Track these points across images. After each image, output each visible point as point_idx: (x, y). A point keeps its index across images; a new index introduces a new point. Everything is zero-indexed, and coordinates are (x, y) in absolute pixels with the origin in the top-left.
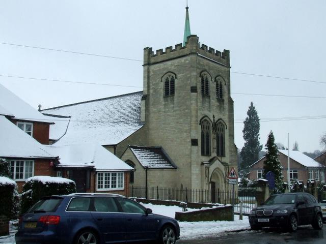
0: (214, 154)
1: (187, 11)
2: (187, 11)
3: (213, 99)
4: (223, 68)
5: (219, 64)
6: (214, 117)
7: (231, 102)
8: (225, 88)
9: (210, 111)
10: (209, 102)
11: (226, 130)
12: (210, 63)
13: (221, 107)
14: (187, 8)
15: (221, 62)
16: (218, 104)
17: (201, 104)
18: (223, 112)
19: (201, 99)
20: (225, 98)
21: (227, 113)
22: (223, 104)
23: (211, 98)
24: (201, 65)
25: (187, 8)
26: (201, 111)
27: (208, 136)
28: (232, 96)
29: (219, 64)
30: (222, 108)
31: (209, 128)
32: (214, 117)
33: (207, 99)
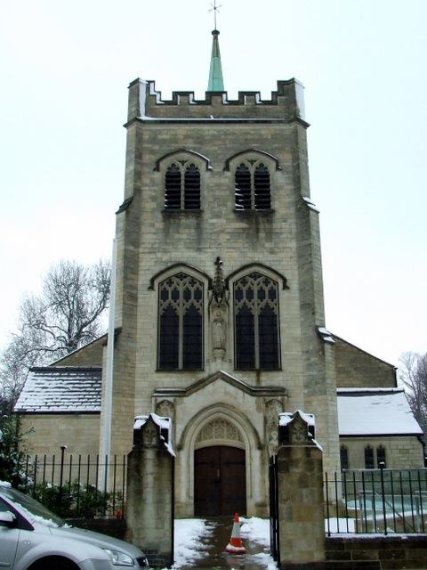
0: (218, 363)
1: (216, 39)
2: (216, 39)
3: (218, 216)
4: (287, 129)
5: (246, 122)
6: (218, 263)
7: (305, 215)
8: (279, 180)
9: (199, 250)
10: (199, 227)
11: (283, 295)
12: (205, 127)
13: (258, 231)
14: (216, 33)
15: (257, 116)
16: (244, 225)
17: (161, 236)
18: (268, 245)
19: (160, 225)
20: (282, 203)
21: (293, 244)
22: (270, 222)
23: (207, 215)
24: (164, 141)
25: (216, 33)
26: (159, 255)
27: (194, 322)
28: (316, 198)
29: (246, 122)
30: (262, 235)
31: (199, 295)
32: (218, 263)
33: (187, 221)
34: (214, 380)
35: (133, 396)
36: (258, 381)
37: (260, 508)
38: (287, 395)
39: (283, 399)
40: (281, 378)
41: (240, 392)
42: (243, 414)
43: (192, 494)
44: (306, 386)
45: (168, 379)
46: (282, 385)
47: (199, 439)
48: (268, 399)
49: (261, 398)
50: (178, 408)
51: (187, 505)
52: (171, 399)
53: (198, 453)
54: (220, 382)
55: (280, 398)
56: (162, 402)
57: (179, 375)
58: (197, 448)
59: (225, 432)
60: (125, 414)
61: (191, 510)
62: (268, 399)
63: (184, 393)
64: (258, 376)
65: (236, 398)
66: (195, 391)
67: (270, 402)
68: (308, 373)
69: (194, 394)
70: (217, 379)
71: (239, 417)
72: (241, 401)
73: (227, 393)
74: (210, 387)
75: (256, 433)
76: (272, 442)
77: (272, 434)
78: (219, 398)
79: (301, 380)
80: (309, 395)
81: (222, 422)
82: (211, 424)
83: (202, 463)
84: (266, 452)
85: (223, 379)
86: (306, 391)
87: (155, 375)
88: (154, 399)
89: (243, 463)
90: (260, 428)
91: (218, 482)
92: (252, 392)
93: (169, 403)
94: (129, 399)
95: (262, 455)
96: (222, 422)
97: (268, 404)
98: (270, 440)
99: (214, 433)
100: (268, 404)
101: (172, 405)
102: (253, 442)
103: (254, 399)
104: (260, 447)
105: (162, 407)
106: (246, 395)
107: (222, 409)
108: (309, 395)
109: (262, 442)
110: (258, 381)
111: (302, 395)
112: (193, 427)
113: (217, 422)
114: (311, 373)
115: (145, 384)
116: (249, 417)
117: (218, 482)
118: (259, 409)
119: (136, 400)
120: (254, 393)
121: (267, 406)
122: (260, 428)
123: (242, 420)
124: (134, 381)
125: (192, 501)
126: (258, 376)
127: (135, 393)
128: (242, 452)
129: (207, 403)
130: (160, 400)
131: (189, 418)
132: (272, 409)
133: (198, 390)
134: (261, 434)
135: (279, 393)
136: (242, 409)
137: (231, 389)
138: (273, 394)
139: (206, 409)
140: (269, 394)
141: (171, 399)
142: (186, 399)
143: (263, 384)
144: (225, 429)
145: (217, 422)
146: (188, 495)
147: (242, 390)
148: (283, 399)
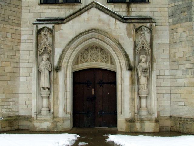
34: (89, 9)
35: (19, 25)
36: (128, 11)
37: (130, 124)
38: (155, 22)
39: (151, 26)
40: (148, 9)
41: (113, 20)
42: (115, 39)
43: (70, 109)
44: (171, 16)
45: (50, 11)
46: (150, 15)
47: (76, 62)
48: (138, 25)
49: (132, 25)
50: (57, 34)
51: (64, 120)
52: (50, 26)
53: (76, 75)
54: (94, 11)
55: (148, 25)
56: (42, 29)
57: (59, 7)
58: (75, 70)
59: (99, 57)
60: (10, 40)
61: (68, 124)
62: (138, 25)
63: (62, 21)
64: (128, 7)
65: (109, 25)
66: (72, 19)
67: (139, 29)
68: (173, 5)
69: (71, 21)
70: (91, 8)
71: (111, 42)
72: (113, 27)
73: (100, 20)
74: (85, 15)
75: (126, 55)
76: (141, 64)
77: (141, 57)
78: (94, 24)
79: (166, 11)
80: (174, 23)
81: (97, 48)
82: (87, 50)
83: (80, 83)
84: (136, 73)
85: (96, 8)
86: (171, 20)
87: (38, 7)
88: (35, 26)
89: (115, 83)
90: (130, 52)
91: (93, 99)
92: (123, 20)
93: (49, 29)
94: (15, 28)
95: (132, 76)
96: (97, 48)
97: (138, 30)
98: (139, 63)
99: (89, 57)
100: (138, 30)
101: (51, 31)
102: (124, 63)
103: (125, 25)
104: (130, 69)
105: (42, 33)
106: (118, 22)
107: (95, 34)
108: (174, 23)
109: (132, 64)
110: (128, 11)
111: (168, 24)
112: (69, 51)
113: (92, 48)
114: (176, 4)
115: (30, 15)
116: (121, 42)
117: (93, 99)
118: (129, 34)
119: (22, 29)
120: (125, 21)
121: (136, 31)
122: (130, 52)
123: (114, 44)
124: (21, 13)
125: (69, 116)
126: (128, 7)
127: (22, 23)
128: (114, 74)
129: (82, 30)
130: (40, 26)
131: (67, 42)
132: (141, 35)
133: (76, 17)
134: (131, 57)
135: (148, 21)
136: (114, 34)
137: (105, 16)
138: (142, 21)
139: (81, 34)
140: (139, 21)
141: (50, 26)
142: (63, 26)
143: (133, 14)
144: (99, 54)
145: (92, 48)
146: (65, 111)
147: (114, 17)
148: (151, 26)
